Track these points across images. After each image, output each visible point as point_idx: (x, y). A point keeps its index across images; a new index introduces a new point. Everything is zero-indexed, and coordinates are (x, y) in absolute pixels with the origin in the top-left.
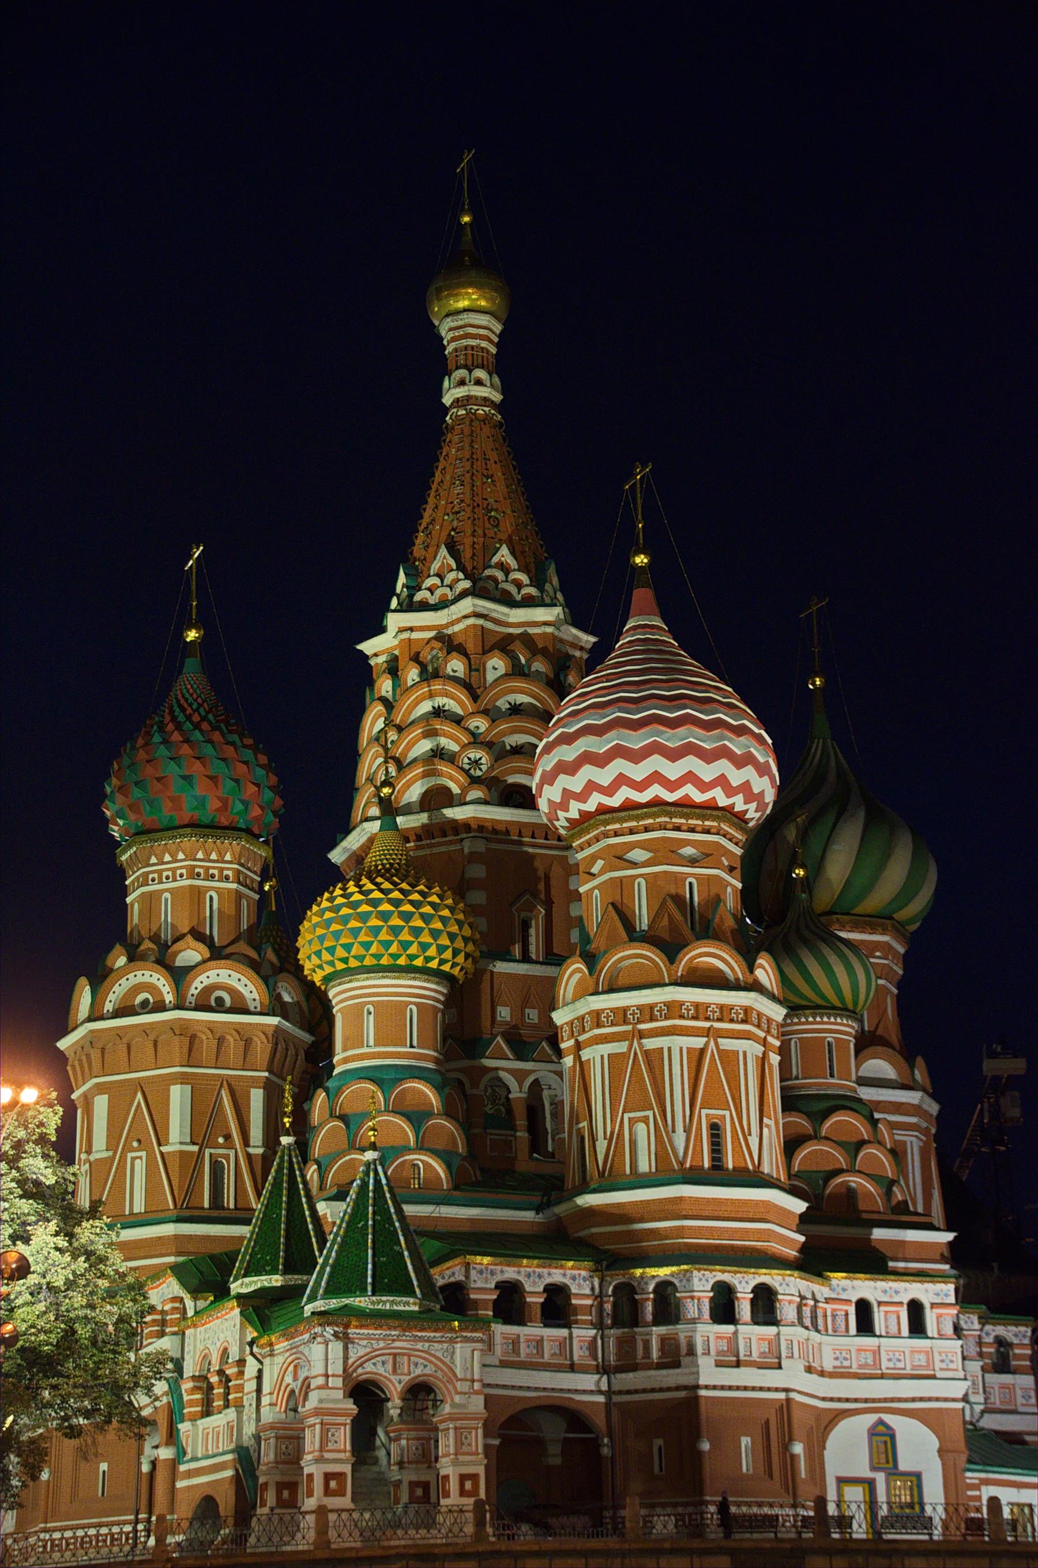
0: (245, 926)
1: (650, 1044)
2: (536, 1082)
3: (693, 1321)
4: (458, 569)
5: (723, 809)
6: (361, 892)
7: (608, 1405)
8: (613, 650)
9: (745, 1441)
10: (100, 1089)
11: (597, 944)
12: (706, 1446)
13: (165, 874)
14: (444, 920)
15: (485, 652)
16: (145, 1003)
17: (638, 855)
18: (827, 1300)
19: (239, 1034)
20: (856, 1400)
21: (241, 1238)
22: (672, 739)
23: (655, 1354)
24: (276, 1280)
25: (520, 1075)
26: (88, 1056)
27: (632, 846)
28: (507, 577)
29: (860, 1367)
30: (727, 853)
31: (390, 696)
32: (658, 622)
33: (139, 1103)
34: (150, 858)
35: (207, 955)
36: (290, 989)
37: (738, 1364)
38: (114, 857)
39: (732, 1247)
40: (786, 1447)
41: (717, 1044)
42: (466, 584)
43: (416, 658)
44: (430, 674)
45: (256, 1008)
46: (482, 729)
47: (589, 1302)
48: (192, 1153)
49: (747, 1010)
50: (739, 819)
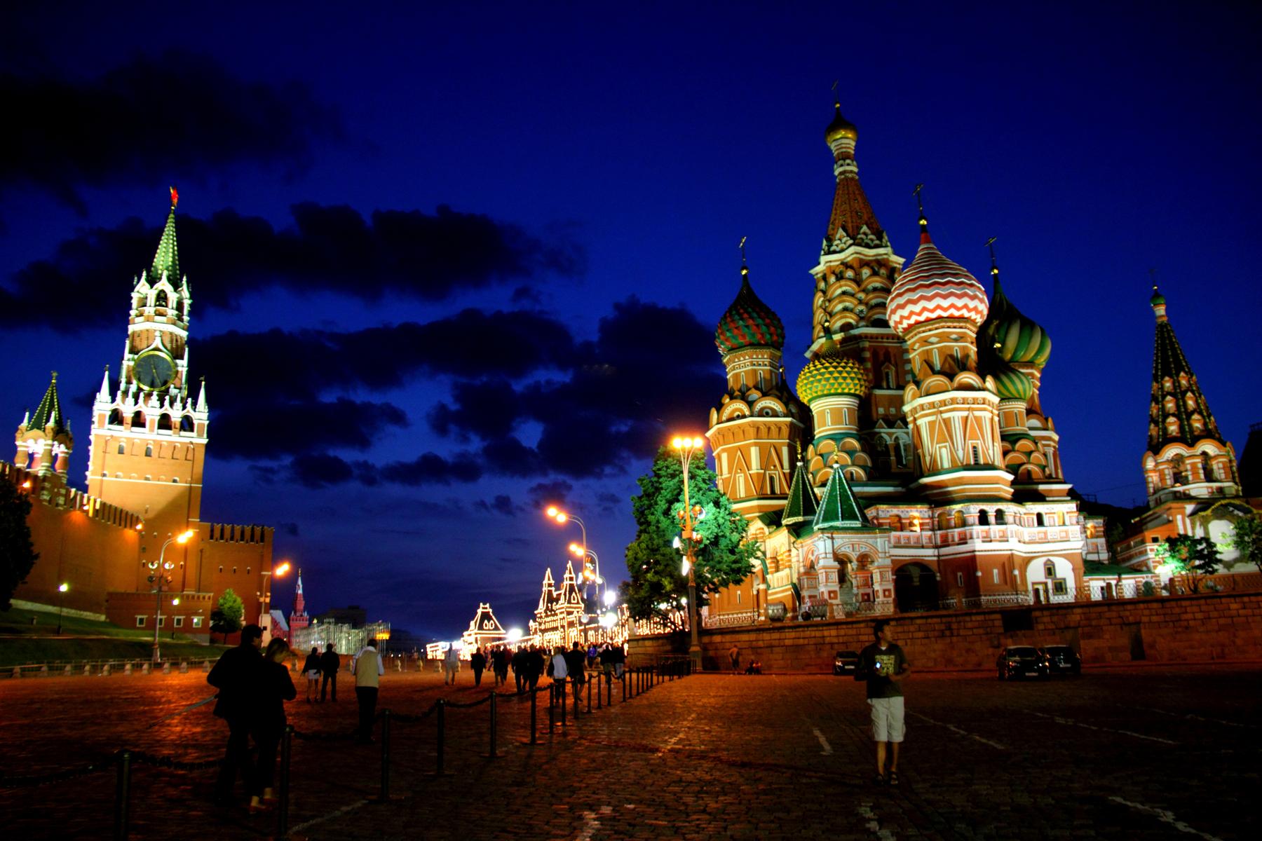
0: (774, 383)
1: (945, 416)
2: (897, 438)
3: (972, 525)
7: (938, 561)
9: (995, 571)
10: (724, 450)
11: (920, 377)
12: (979, 574)
14: (855, 373)
17: (933, 340)
18: (1025, 514)
21: (784, 505)
23: (956, 539)
24: (800, 519)
25: (890, 435)
27: (931, 336)
30: (971, 337)
37: (991, 541)
38: (721, 361)
39: (985, 495)
42: (851, 242)
43: (833, 273)
44: (840, 277)
47: (927, 521)
49: (984, 399)
50: (973, 322)
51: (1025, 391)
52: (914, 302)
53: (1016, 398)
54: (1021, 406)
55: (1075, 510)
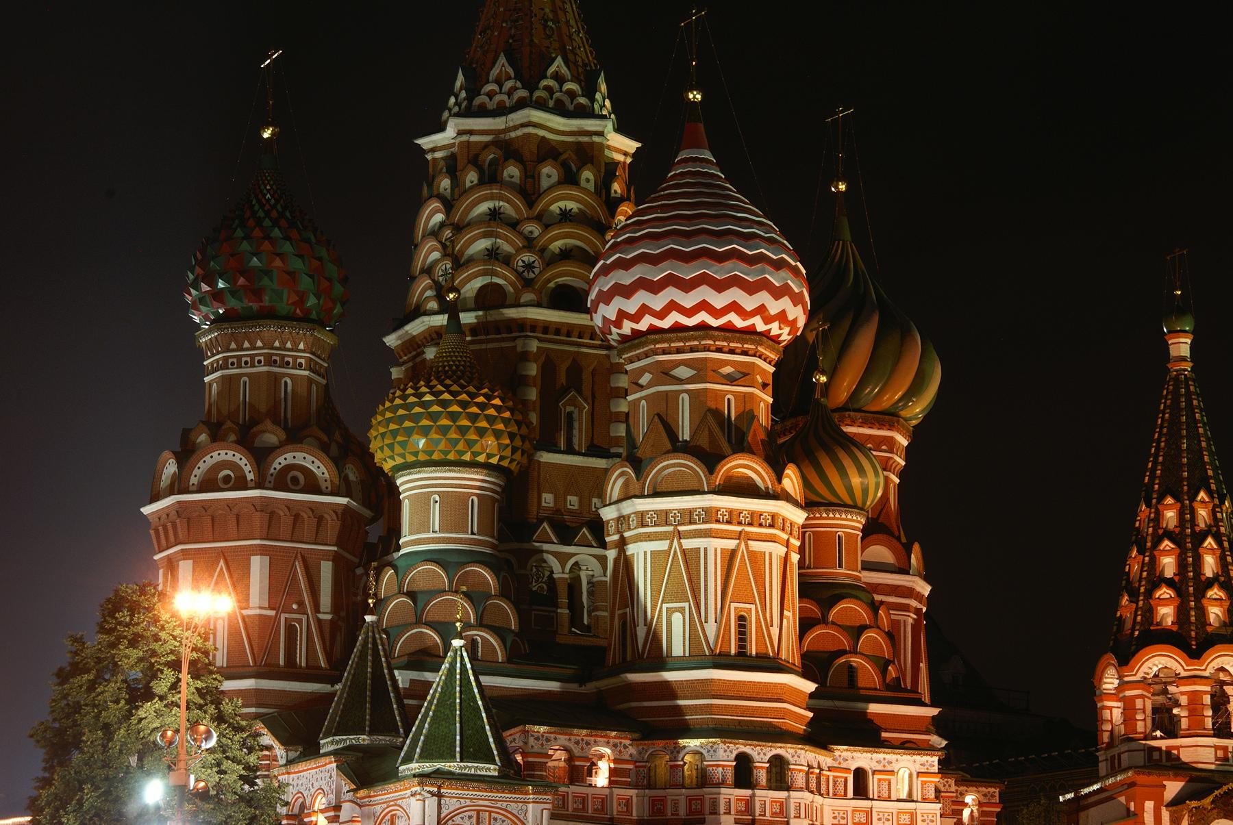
1: (688, 544)
2: (576, 564)
4: (516, 78)
5: (761, 334)
6: (432, 393)
13: (244, 359)
14: (506, 422)
16: (227, 478)
17: (683, 372)
18: (830, 769)
19: (313, 512)
24: (364, 739)
25: (563, 558)
28: (561, 88)
30: (764, 371)
31: (448, 193)
32: (708, 155)
35: (283, 436)
36: (354, 470)
38: (195, 339)
41: (747, 545)
42: (523, 93)
43: (475, 162)
45: (327, 488)
46: (536, 233)
48: (271, 616)
50: (775, 340)
51: (865, 491)
52: (655, 288)
54: (853, 523)
55: (935, 769)
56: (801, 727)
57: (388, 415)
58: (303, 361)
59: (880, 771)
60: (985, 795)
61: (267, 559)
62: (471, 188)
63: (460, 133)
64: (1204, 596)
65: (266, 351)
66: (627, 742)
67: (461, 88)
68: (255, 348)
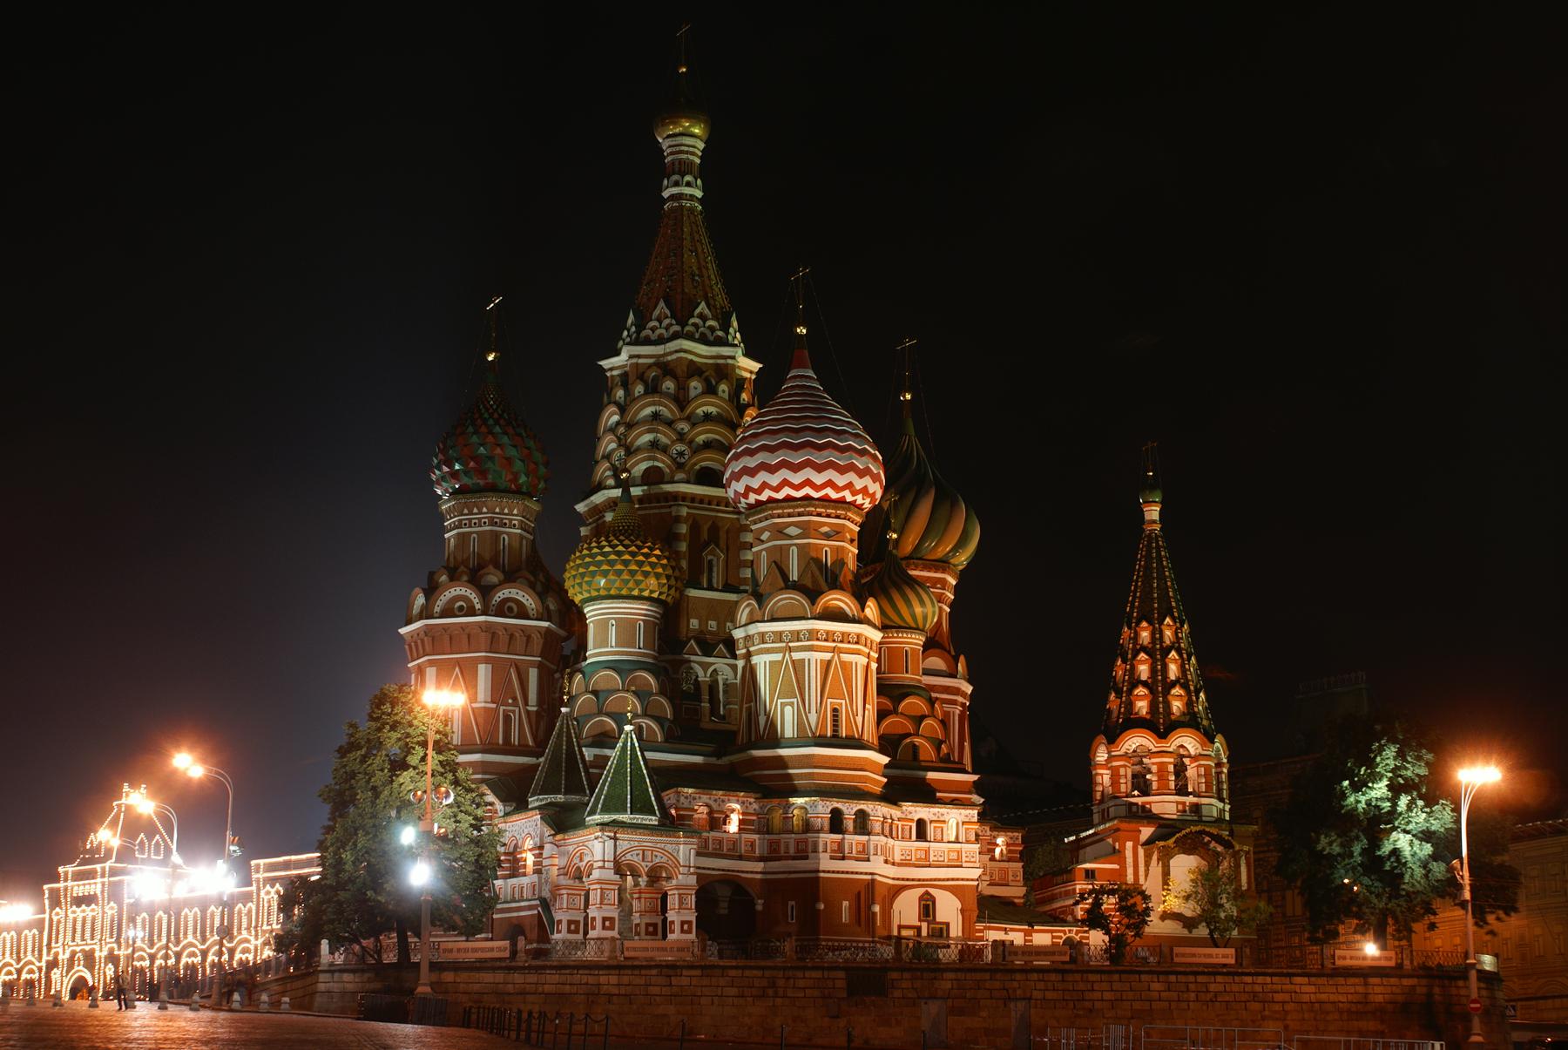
1: (797, 656)
2: (715, 670)
4: (671, 317)
5: (849, 503)
6: (610, 546)
8: (779, 391)
9: (845, 904)
12: (822, 906)
14: (664, 566)
15: (690, 376)
16: (461, 608)
17: (793, 531)
18: (899, 820)
20: (913, 880)
22: (819, 457)
23: (792, 851)
24: (560, 798)
25: (705, 666)
26: (422, 641)
28: (704, 323)
29: (917, 860)
30: (851, 531)
32: (811, 373)
33: (457, 674)
34: (463, 510)
35: (502, 577)
37: (843, 858)
38: (437, 507)
40: (869, 907)
41: (839, 657)
42: (677, 328)
43: (641, 378)
47: (754, 818)
48: (492, 708)
49: (859, 636)
50: (860, 507)
51: (925, 618)
52: (772, 469)
53: (911, 628)
54: (916, 641)
55: (976, 819)
56: (878, 789)
57: (578, 562)
58: (516, 522)
59: (936, 821)
60: (1011, 838)
61: (490, 666)
62: (638, 397)
63: (631, 357)
64: (1169, 693)
65: (490, 515)
66: (752, 800)
67: (632, 324)
68: (481, 513)
